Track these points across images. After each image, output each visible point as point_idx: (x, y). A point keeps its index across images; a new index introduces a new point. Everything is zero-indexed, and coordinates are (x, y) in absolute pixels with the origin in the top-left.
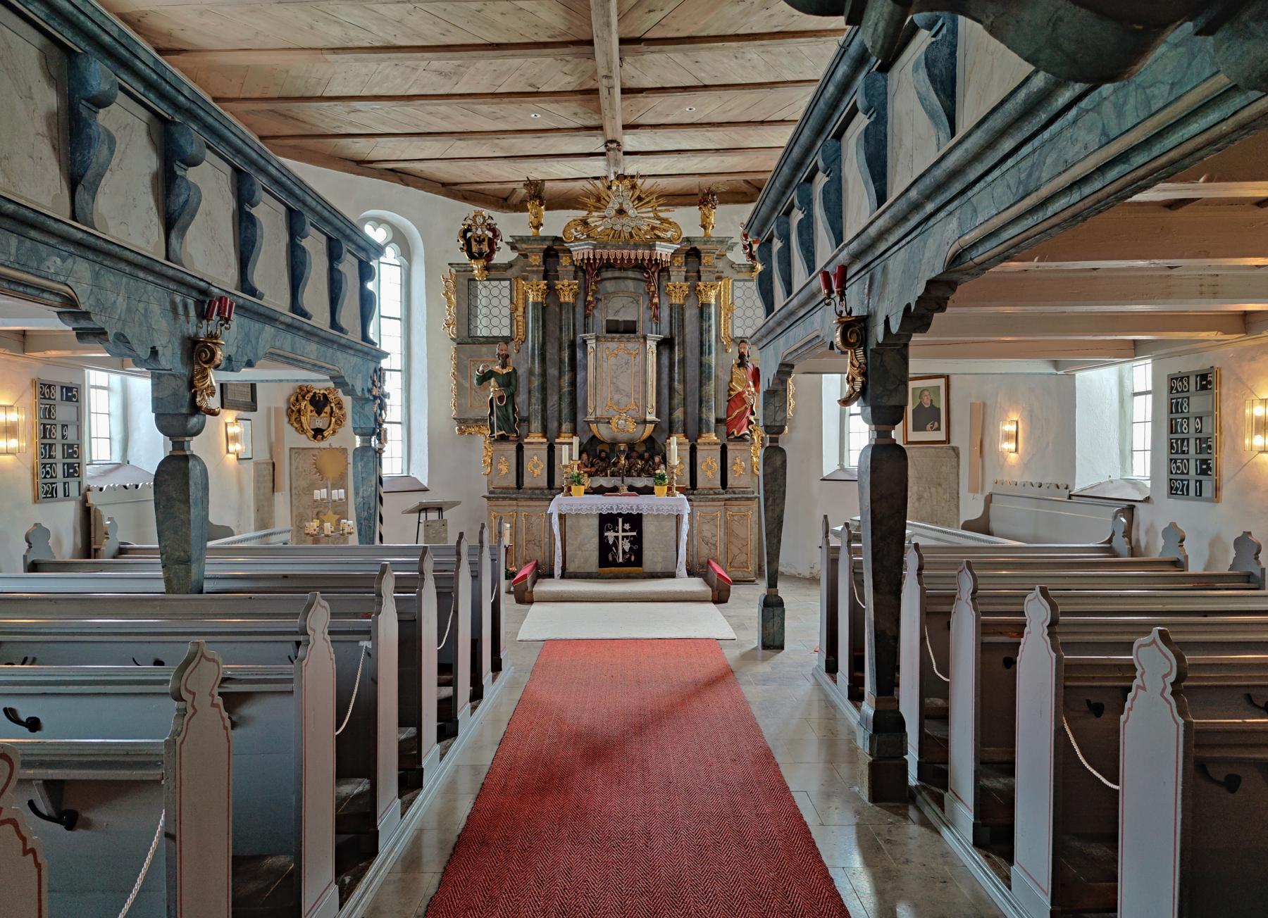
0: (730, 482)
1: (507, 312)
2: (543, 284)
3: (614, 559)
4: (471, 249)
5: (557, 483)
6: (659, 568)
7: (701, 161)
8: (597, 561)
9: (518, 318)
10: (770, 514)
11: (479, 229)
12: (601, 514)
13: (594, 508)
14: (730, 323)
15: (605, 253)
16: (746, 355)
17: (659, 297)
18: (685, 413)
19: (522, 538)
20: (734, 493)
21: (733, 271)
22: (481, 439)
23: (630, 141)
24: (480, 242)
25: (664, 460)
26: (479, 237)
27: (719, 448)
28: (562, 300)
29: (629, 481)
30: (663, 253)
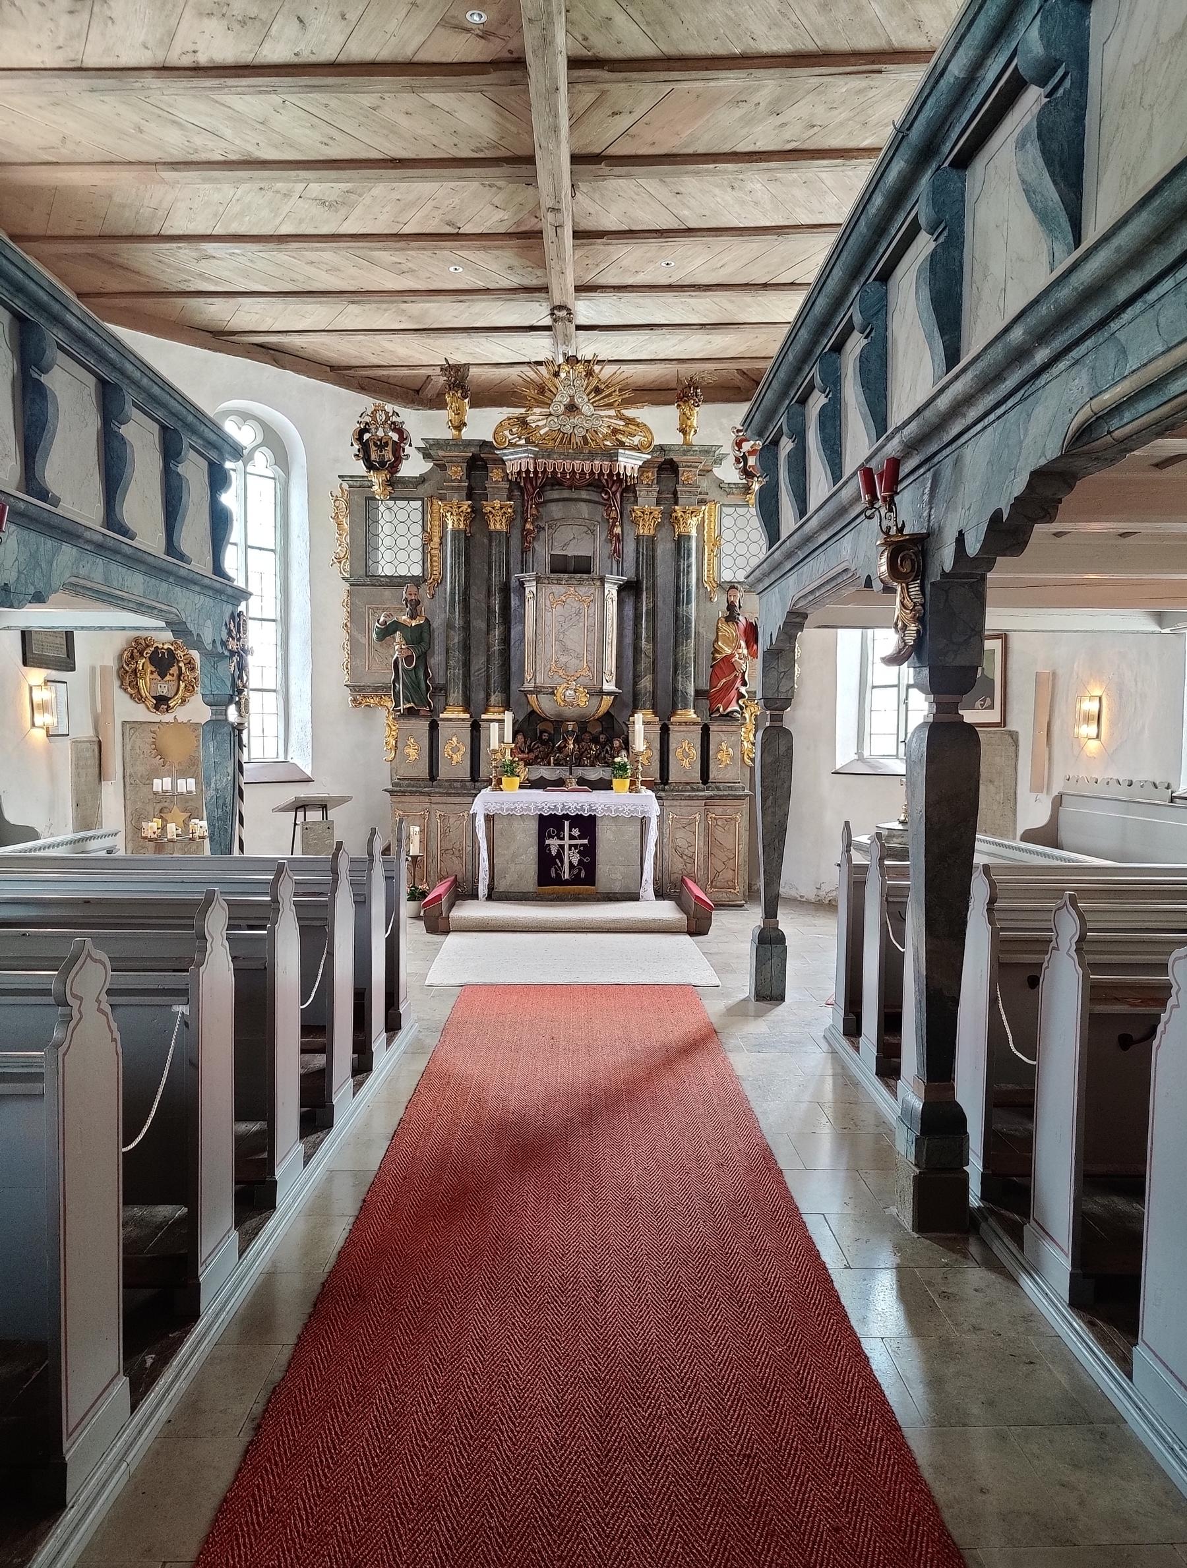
0: (713, 774)
1: (417, 542)
2: (466, 505)
3: (558, 875)
4: (369, 456)
5: (484, 773)
6: (617, 888)
7: (681, 341)
8: (536, 878)
9: (432, 551)
10: (769, 819)
11: (381, 430)
12: (541, 815)
14: (715, 562)
15: (550, 464)
16: (737, 605)
17: (622, 525)
18: (654, 681)
19: (436, 846)
20: (718, 789)
21: (721, 492)
22: (383, 715)
23: (586, 310)
24: (382, 445)
25: (626, 745)
26: (380, 440)
27: (699, 728)
28: (492, 527)
29: (579, 771)
30: (627, 465)
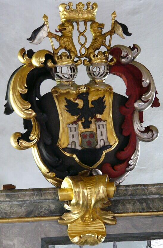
4: (55, 137)
11: (82, 69)
26: (83, 96)
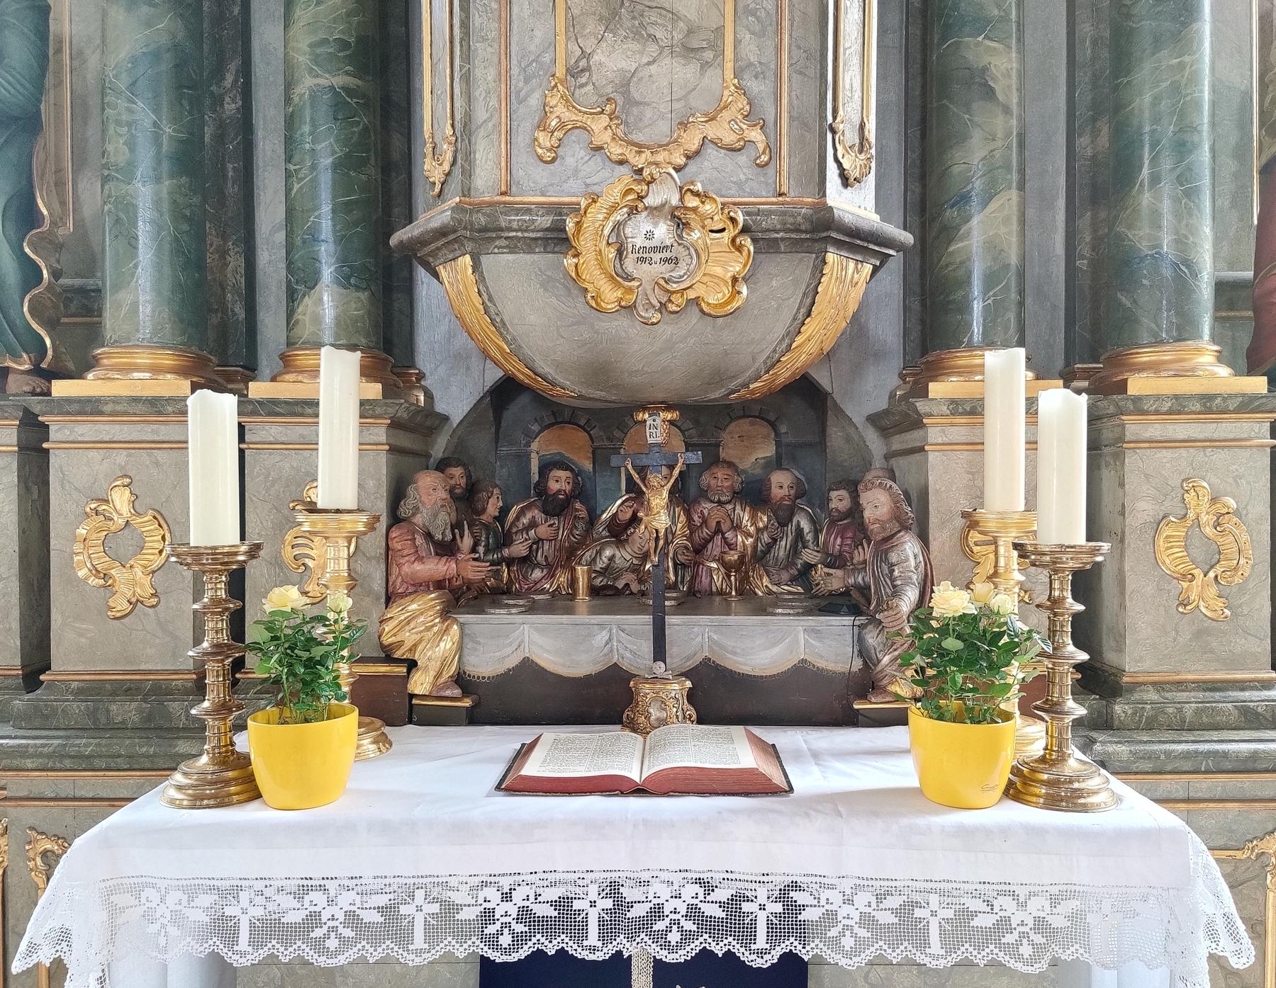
13: (419, 912)
